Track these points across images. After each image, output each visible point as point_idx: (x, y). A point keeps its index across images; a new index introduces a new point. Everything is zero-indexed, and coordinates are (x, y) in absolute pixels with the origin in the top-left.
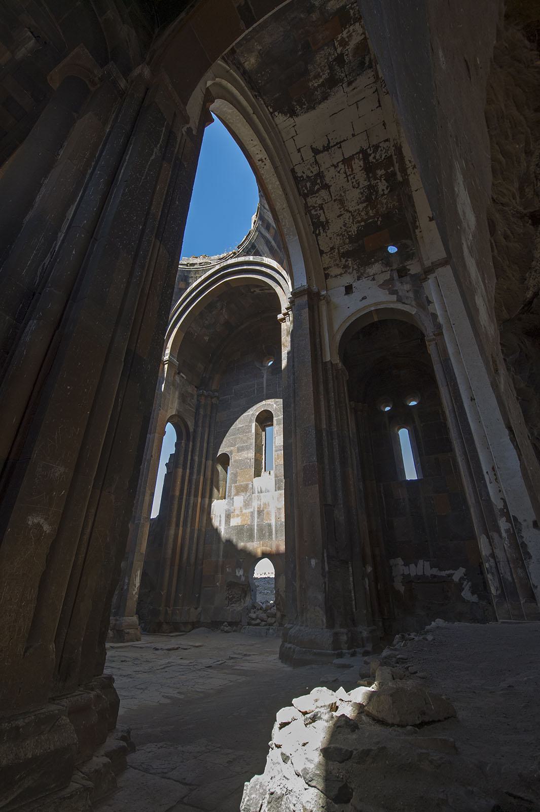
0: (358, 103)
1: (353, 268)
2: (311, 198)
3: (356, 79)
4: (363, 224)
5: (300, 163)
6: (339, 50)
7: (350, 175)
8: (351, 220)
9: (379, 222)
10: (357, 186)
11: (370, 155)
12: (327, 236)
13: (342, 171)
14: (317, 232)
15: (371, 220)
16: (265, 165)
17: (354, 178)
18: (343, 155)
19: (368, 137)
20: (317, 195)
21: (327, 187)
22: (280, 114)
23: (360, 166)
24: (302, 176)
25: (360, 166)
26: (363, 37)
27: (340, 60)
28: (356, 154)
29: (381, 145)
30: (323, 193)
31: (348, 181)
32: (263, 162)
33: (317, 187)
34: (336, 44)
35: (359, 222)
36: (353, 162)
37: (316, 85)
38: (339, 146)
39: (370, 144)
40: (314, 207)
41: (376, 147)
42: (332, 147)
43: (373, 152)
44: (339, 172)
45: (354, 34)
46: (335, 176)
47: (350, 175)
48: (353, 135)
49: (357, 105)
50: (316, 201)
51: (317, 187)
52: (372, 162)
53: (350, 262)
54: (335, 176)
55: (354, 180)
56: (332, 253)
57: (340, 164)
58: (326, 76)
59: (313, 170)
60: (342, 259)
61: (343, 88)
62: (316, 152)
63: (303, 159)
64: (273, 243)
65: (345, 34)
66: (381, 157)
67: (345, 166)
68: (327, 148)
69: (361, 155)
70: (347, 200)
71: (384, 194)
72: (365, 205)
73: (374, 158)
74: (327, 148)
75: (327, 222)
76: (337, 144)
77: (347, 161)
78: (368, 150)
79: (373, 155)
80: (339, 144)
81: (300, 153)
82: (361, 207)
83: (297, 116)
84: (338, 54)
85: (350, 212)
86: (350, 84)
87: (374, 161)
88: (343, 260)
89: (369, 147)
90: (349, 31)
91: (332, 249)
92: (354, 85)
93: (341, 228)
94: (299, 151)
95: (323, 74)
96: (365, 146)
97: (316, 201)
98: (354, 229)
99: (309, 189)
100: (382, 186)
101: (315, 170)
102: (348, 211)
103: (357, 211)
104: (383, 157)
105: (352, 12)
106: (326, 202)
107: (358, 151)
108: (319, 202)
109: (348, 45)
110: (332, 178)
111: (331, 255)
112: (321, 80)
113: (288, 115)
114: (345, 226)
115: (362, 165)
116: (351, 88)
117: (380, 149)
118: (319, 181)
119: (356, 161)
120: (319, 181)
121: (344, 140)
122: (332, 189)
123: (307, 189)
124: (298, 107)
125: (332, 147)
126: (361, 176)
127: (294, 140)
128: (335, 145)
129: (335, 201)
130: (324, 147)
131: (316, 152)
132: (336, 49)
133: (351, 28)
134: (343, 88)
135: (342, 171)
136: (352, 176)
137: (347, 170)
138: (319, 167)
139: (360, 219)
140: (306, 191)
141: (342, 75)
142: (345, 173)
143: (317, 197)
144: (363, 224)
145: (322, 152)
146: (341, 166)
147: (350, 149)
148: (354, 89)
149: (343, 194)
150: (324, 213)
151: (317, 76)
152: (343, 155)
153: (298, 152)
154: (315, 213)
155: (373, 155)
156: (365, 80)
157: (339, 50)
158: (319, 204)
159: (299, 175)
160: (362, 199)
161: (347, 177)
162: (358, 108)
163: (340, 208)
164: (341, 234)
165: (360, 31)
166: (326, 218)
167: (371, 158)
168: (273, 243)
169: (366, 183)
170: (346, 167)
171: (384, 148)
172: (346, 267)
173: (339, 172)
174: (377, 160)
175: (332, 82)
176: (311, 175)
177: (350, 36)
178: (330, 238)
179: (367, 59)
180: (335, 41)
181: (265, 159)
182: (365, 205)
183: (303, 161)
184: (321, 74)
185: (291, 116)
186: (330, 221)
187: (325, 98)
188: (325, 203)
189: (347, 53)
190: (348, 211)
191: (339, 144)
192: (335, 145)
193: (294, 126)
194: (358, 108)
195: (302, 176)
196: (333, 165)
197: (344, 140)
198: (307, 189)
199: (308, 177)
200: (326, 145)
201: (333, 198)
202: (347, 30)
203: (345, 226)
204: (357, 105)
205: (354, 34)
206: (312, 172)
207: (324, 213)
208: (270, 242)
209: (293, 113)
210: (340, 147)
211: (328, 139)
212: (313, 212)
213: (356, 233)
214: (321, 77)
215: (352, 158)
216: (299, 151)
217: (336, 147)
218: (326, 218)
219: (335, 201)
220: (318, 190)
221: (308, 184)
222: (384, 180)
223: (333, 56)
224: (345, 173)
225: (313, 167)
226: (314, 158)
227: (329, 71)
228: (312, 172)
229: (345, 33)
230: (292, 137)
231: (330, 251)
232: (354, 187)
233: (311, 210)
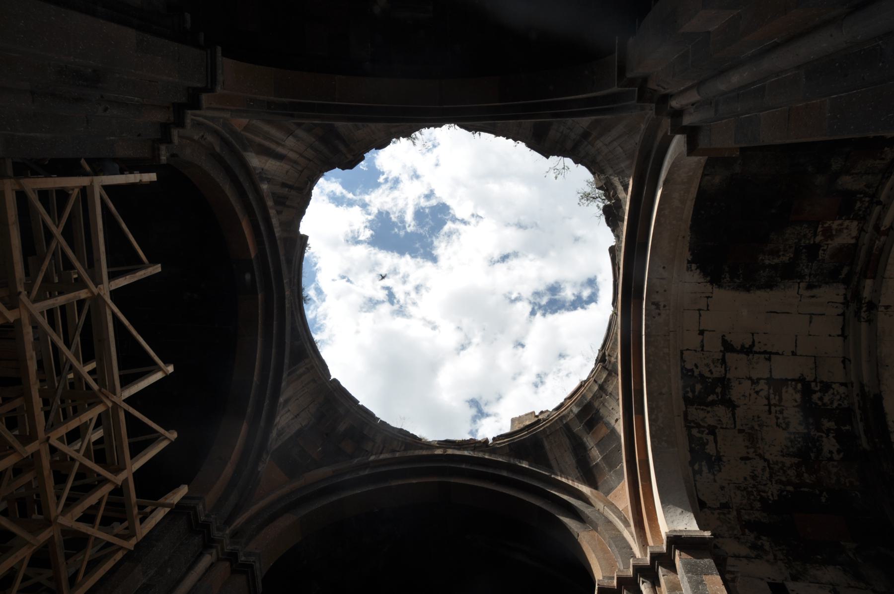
0: (812, 316)
1: (775, 556)
2: (696, 409)
3: (820, 287)
4: (790, 488)
5: (695, 351)
6: (819, 238)
7: (775, 405)
8: (767, 474)
9: (823, 500)
10: (784, 426)
11: (815, 392)
12: (715, 481)
13: (763, 393)
14: (696, 467)
15: (806, 490)
16: (659, 314)
17: (781, 412)
18: (771, 372)
19: (816, 367)
20: (709, 409)
21: (731, 405)
22: (698, 271)
23: (796, 401)
24: (692, 371)
25: (796, 401)
26: (853, 241)
27: (813, 250)
28: (793, 380)
29: (834, 386)
30: (721, 411)
31: (770, 412)
33: (711, 398)
34: (820, 229)
35: (779, 482)
36: (784, 390)
37: (767, 262)
38: (767, 356)
39: (816, 378)
40: (698, 426)
41: (826, 387)
42: (756, 353)
43: (820, 391)
44: (757, 393)
45: (845, 231)
46: (750, 395)
47: (775, 405)
48: (794, 354)
49: (811, 318)
50: (705, 417)
51: (711, 398)
52: (816, 404)
53: (765, 542)
54: (750, 395)
55: (780, 416)
56: (724, 514)
57: (762, 382)
58: (786, 259)
59: (713, 370)
60: (747, 531)
61: (799, 288)
62: (728, 347)
63: (702, 346)
65: (835, 225)
66: (832, 403)
67: (769, 389)
68: (748, 350)
69: (799, 386)
70: (762, 439)
71: (831, 459)
72: (796, 460)
73: (821, 399)
74: (748, 350)
75: (719, 459)
76: (765, 352)
77: (778, 385)
78: (813, 384)
79: (819, 394)
80: (769, 355)
81: (700, 337)
82: (788, 461)
83: (720, 286)
84: (814, 242)
85: (765, 460)
86: (810, 287)
87: (820, 403)
88: (751, 537)
89: (815, 381)
90: (841, 225)
91: (725, 506)
92: (815, 292)
93: (745, 479)
94: (701, 332)
95: (783, 255)
97: (705, 417)
98: (772, 491)
99: (697, 393)
100: (830, 445)
101: (718, 371)
102: (761, 457)
103: (780, 465)
104: (835, 405)
105: (858, 204)
106: (724, 426)
107: (797, 376)
108: (711, 421)
109: (832, 240)
110: (743, 396)
111: (722, 516)
112: (776, 261)
113: (708, 279)
114: (754, 477)
115: (799, 400)
117: (831, 391)
118: (719, 390)
119: (791, 390)
120: (719, 390)
121: (777, 353)
122: (739, 412)
123: (693, 391)
124: (727, 275)
125: (756, 353)
126: (794, 416)
127: (700, 315)
128: (760, 353)
129: (741, 431)
130: (743, 346)
131: (728, 347)
132: (815, 235)
133: (847, 223)
134: (799, 288)
136: (778, 408)
137: (772, 396)
138: (726, 371)
139: (784, 479)
140: (690, 395)
141: (806, 270)
142: (768, 398)
143: (708, 412)
144: (790, 488)
145: (738, 352)
146: (762, 385)
148: (813, 297)
149: (757, 427)
150: (716, 442)
152: (771, 372)
153: (699, 334)
154: (698, 435)
155: (819, 394)
157: (819, 238)
158: (709, 425)
159: (689, 366)
160: (791, 449)
161: (769, 405)
162: (810, 322)
163: (747, 447)
164: (745, 489)
165: (854, 233)
166: (718, 452)
167: (815, 397)
169: (802, 429)
170: (771, 391)
171: (838, 393)
172: (754, 547)
173: (757, 393)
174: (824, 404)
175: (789, 273)
176: (708, 375)
177: (840, 231)
178: (722, 488)
179: (845, 270)
180: (820, 226)
182: (796, 460)
183: (702, 350)
184: (781, 253)
185: (711, 282)
186: (724, 459)
187: (770, 285)
188: (722, 428)
189: (825, 248)
190: (761, 457)
191: (769, 355)
192: (760, 353)
193: (708, 297)
194: (810, 322)
195: (692, 371)
196: (750, 378)
197: (777, 353)
198: (693, 391)
199: (701, 375)
200: (747, 346)
201: (738, 427)
202: (839, 222)
203: (754, 477)
204: (811, 318)
205: (845, 231)
206: (710, 371)
207: (716, 442)
209: (715, 280)
210: (769, 359)
211: (753, 342)
212: (695, 432)
213: (776, 498)
214: (779, 256)
215: (785, 382)
216: (701, 332)
217: (763, 356)
218: (718, 452)
219: (741, 431)
220: (713, 403)
221: (698, 387)
222: (833, 437)
223: (807, 242)
224: (768, 398)
225: (716, 366)
226: (721, 354)
227: (792, 256)
228: (710, 371)
230: (699, 310)
231: (718, 509)
232: (778, 425)
233: (693, 427)
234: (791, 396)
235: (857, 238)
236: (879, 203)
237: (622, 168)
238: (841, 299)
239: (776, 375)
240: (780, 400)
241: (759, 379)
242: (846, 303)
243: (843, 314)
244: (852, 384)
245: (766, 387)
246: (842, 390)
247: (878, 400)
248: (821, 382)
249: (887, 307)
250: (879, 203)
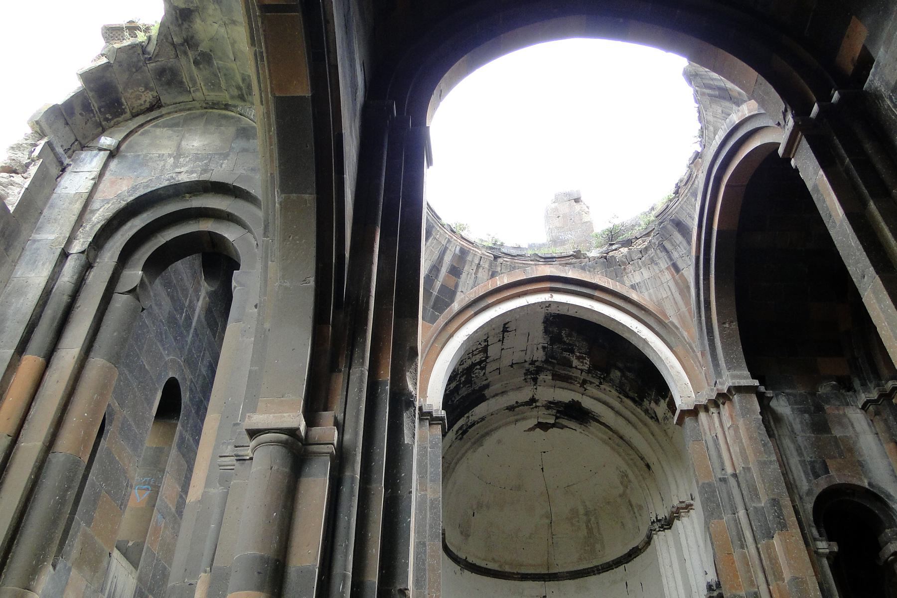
26: (574, 366)
28: (487, 354)
32: (546, 307)
41: (483, 368)
42: (503, 334)
44: (480, 344)
58: (565, 339)
64: (438, 285)
76: (503, 337)
77: (485, 350)
80: (502, 340)
89: (486, 363)
96: (488, 360)
116: (540, 346)
121: (503, 343)
125: (503, 334)
128: (503, 336)
135: (479, 346)
146: (484, 344)
147: (493, 351)
151: (568, 336)
156: (540, 355)
157: (578, 354)
167: (478, 367)
168: (438, 285)
173: (480, 344)
175: (555, 339)
181: (547, 310)
187: (546, 331)
192: (503, 336)
197: (503, 343)
208: (437, 276)
229: (588, 363)
234: (477, 358)
235: (576, 368)
236: (601, 383)
237: (650, 290)
238: (535, 359)
239: (489, 348)
240: (476, 355)
241: (488, 341)
242: (533, 363)
243: (525, 361)
244: (487, 379)
245: (483, 346)
246: (482, 374)
247: (483, 399)
248: (486, 366)
249: (536, 389)
250: (601, 383)
